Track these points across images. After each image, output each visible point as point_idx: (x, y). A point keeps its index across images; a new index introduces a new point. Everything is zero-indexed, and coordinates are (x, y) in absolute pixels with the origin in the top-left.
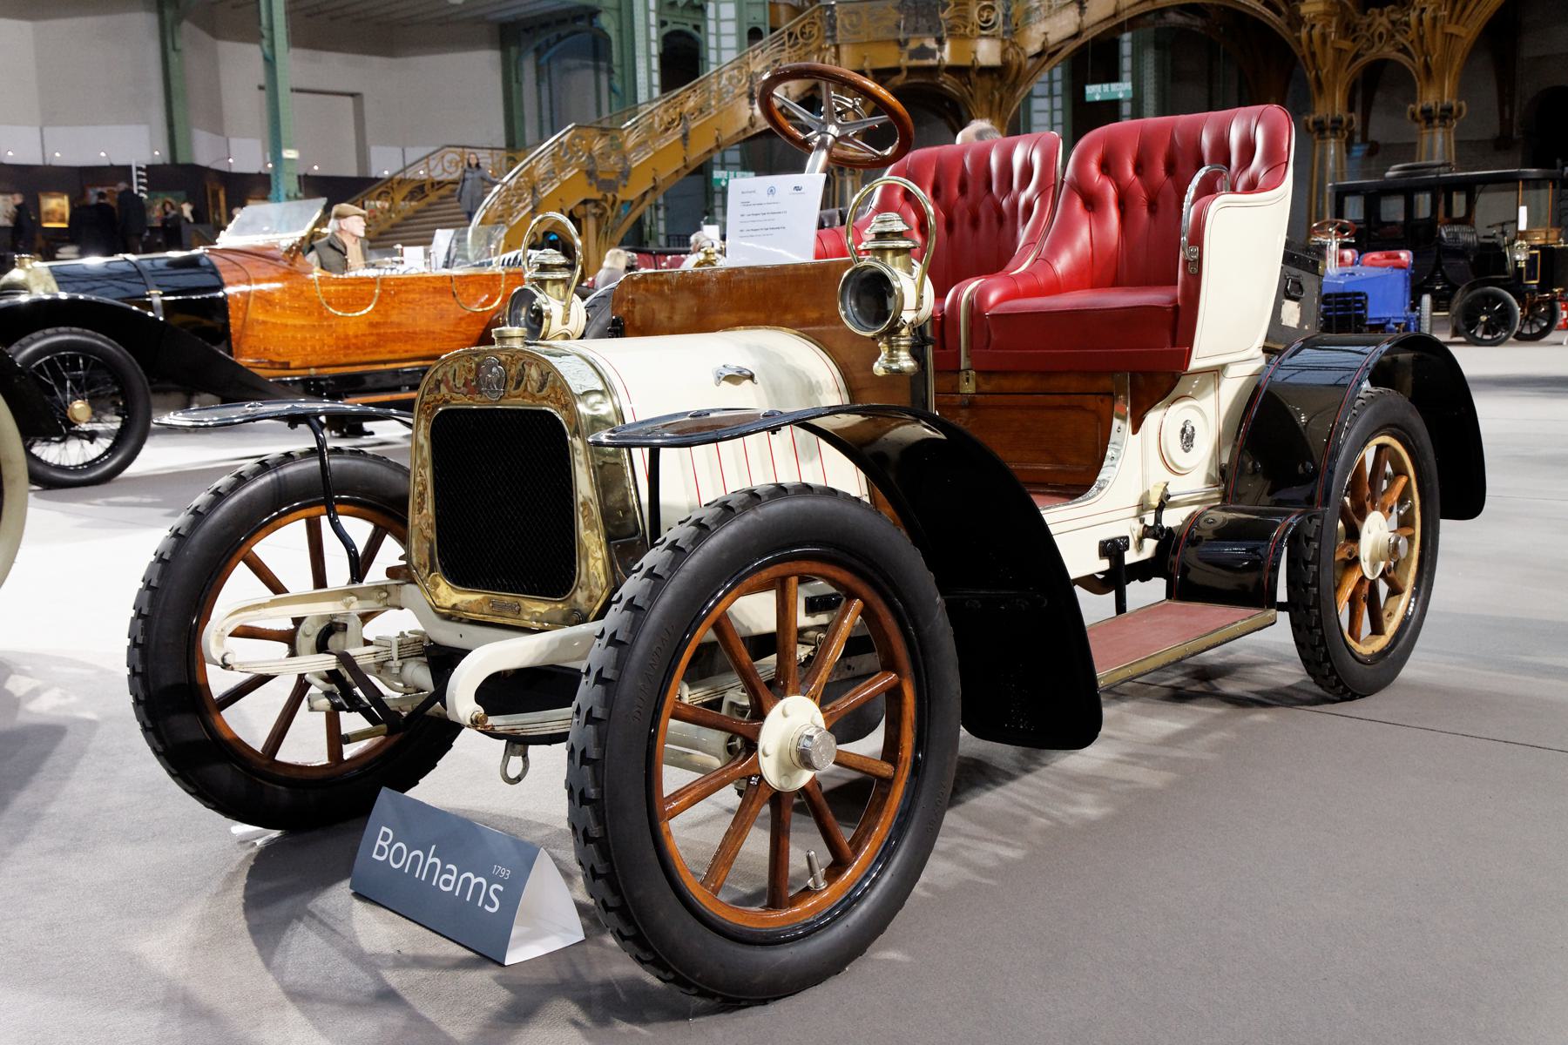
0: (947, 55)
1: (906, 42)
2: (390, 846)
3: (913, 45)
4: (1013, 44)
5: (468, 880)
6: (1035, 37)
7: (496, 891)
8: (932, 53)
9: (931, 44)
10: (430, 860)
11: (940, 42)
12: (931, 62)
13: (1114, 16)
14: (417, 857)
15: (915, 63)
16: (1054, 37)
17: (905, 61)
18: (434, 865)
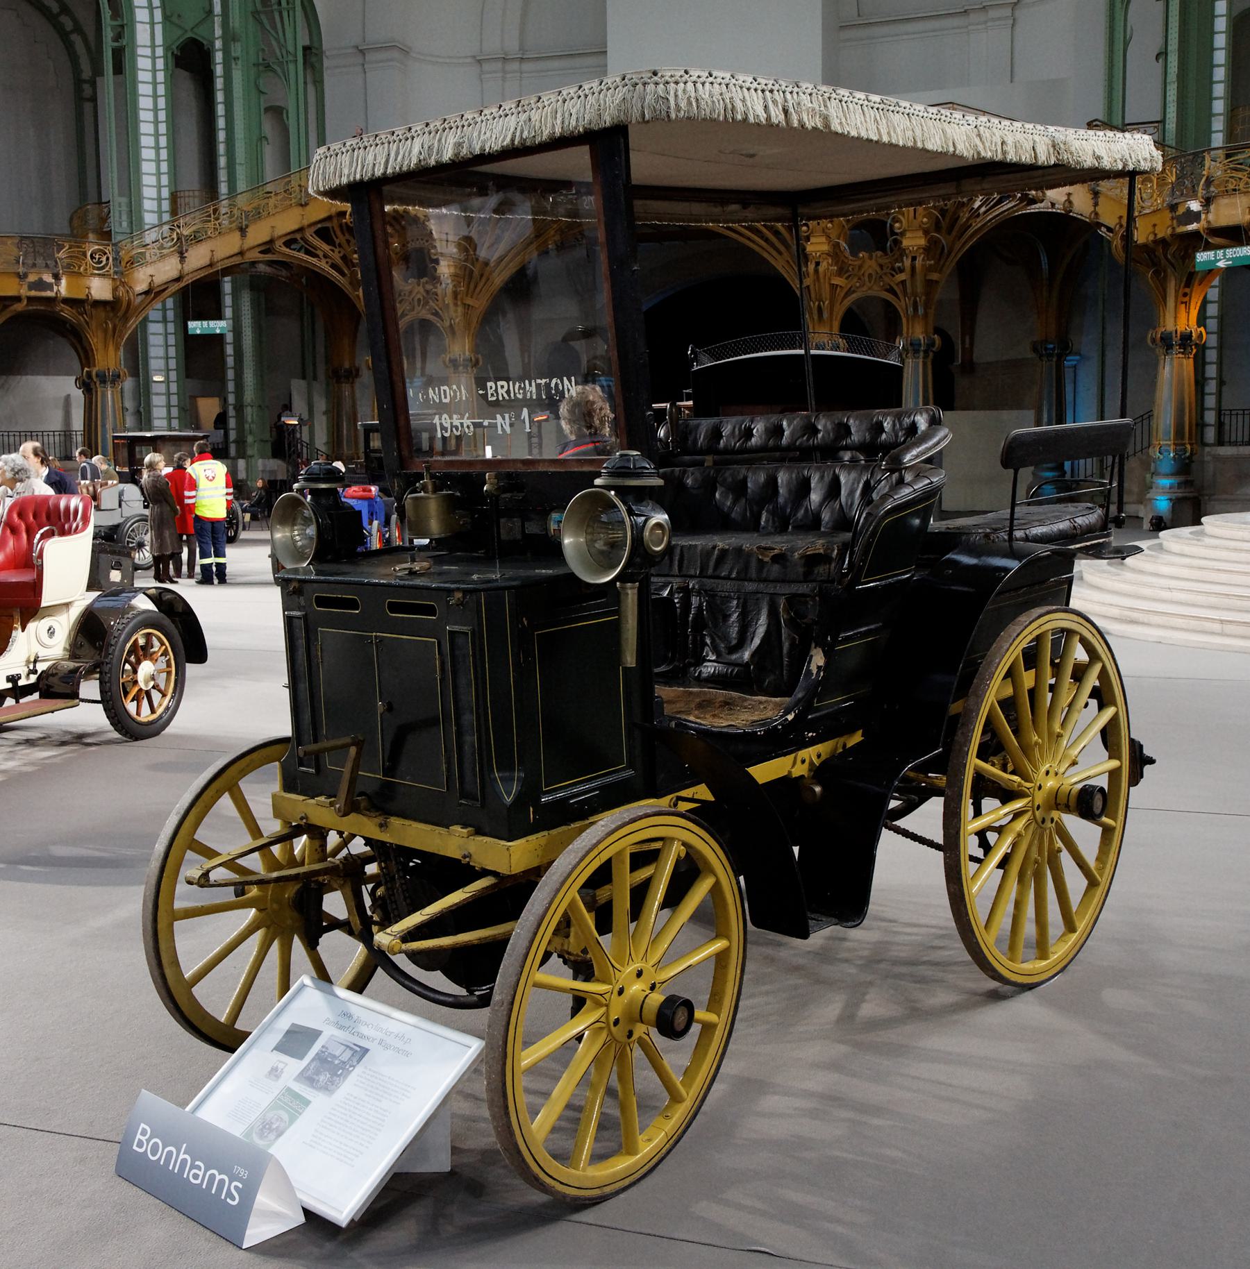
0: (63, 288)
1: (25, 275)
2: (148, 1141)
3: (32, 278)
4: (123, 284)
5: (213, 1176)
6: (141, 279)
7: (236, 1187)
8: (49, 287)
9: (48, 278)
10: (182, 1156)
11: (57, 277)
12: (49, 294)
13: (211, 265)
14: (170, 1153)
15: (33, 293)
16: (159, 279)
17: (24, 292)
18: (184, 1161)
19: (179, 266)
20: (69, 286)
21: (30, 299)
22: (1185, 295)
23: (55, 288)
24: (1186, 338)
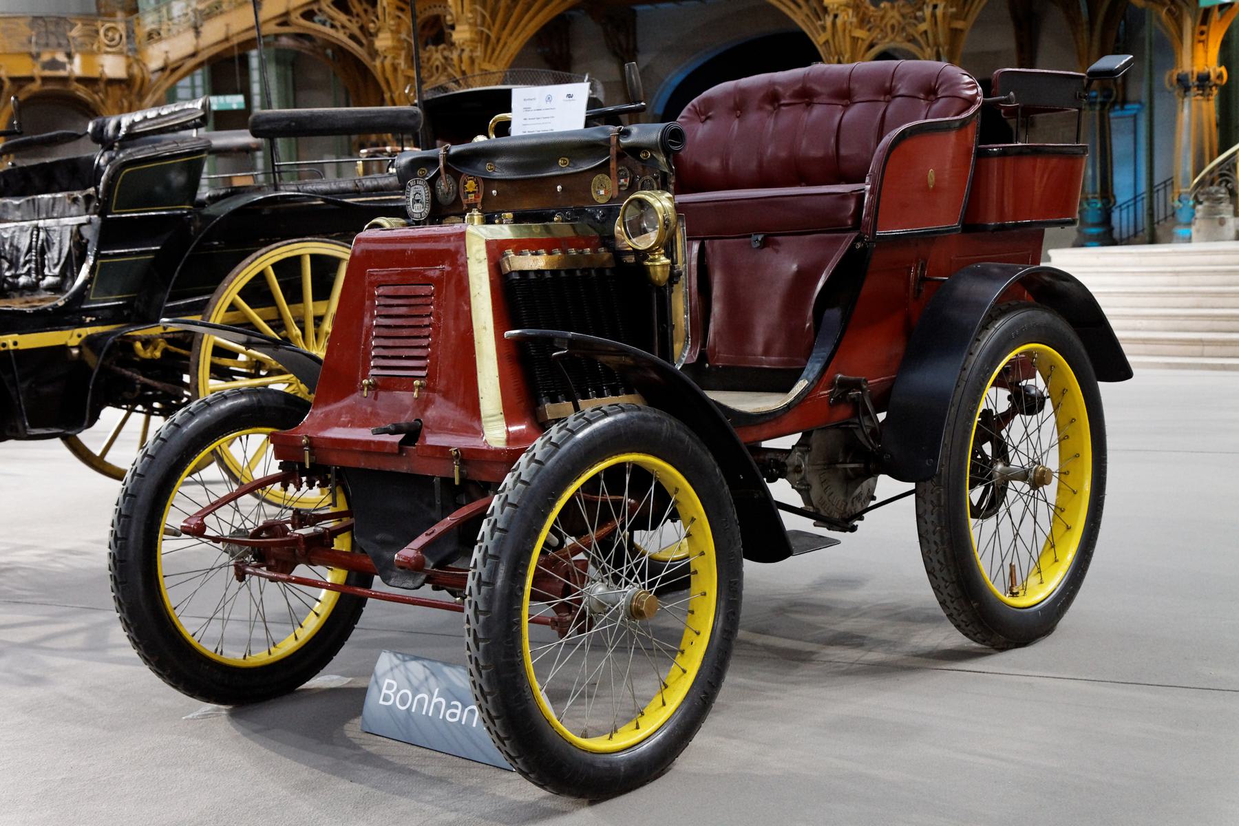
0: (77, 67)
3: (46, 57)
4: (138, 61)
6: (155, 56)
9: (61, 57)
11: (70, 56)
12: (62, 73)
13: (227, 39)
15: (48, 73)
16: (175, 55)
17: (38, 72)
19: (194, 41)
20: (84, 65)
21: (45, 80)
22: (1202, 33)
23: (68, 67)
24: (1204, 79)
